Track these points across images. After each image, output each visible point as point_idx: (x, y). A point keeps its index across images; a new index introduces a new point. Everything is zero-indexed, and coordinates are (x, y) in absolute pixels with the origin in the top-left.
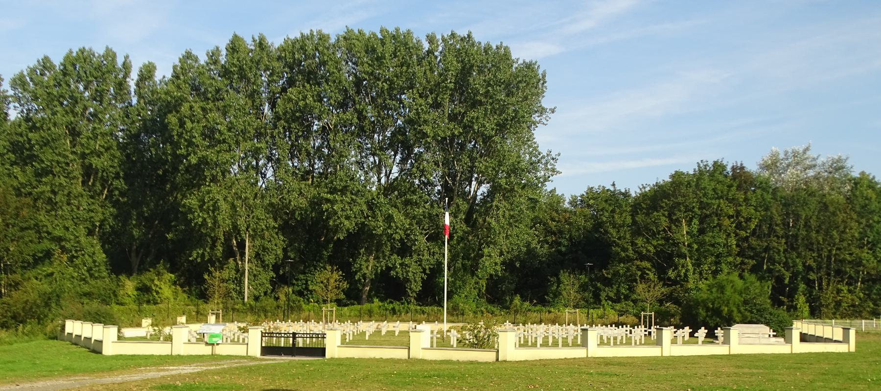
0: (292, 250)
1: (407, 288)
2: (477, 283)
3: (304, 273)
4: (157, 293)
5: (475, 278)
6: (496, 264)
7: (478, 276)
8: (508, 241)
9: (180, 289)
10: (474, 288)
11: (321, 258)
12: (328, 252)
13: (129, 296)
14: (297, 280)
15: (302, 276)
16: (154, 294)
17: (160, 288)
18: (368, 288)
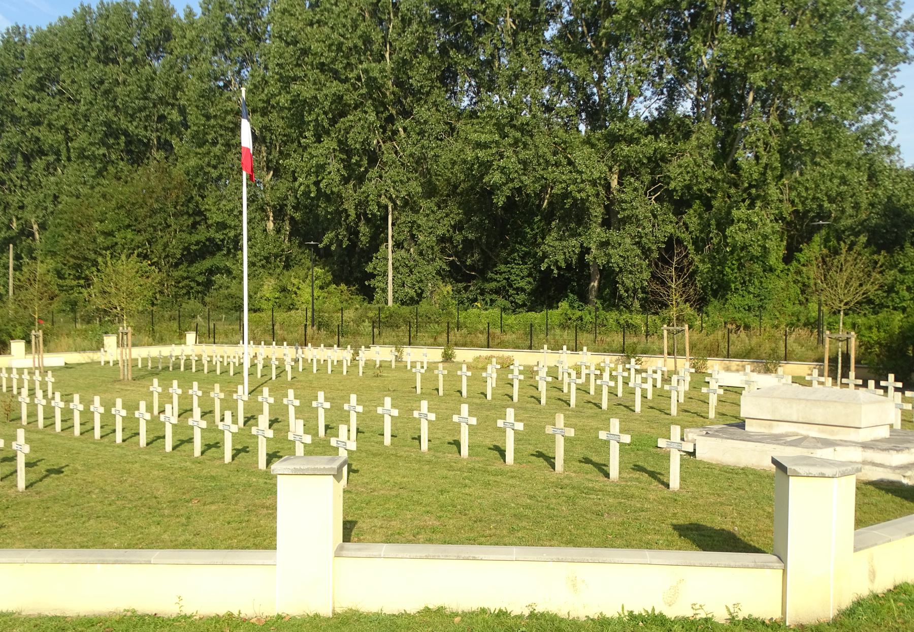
0: (469, 228)
1: (618, 282)
2: (799, 272)
3: (506, 263)
4: (296, 293)
5: (794, 263)
6: (765, 237)
7: (799, 261)
8: (794, 193)
9: (346, 288)
10: (794, 282)
11: (524, 238)
12: (532, 230)
13: (268, 300)
14: (497, 273)
15: (502, 268)
16: (294, 296)
17: (298, 288)
18: (596, 284)
